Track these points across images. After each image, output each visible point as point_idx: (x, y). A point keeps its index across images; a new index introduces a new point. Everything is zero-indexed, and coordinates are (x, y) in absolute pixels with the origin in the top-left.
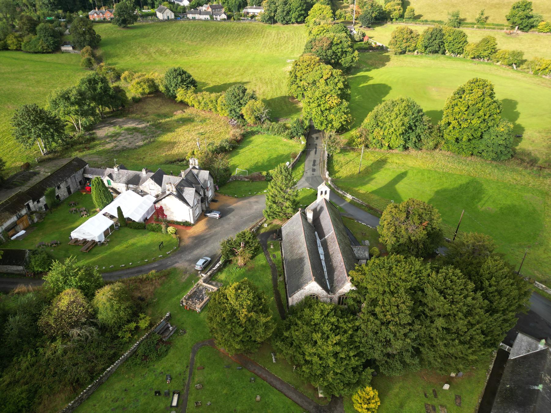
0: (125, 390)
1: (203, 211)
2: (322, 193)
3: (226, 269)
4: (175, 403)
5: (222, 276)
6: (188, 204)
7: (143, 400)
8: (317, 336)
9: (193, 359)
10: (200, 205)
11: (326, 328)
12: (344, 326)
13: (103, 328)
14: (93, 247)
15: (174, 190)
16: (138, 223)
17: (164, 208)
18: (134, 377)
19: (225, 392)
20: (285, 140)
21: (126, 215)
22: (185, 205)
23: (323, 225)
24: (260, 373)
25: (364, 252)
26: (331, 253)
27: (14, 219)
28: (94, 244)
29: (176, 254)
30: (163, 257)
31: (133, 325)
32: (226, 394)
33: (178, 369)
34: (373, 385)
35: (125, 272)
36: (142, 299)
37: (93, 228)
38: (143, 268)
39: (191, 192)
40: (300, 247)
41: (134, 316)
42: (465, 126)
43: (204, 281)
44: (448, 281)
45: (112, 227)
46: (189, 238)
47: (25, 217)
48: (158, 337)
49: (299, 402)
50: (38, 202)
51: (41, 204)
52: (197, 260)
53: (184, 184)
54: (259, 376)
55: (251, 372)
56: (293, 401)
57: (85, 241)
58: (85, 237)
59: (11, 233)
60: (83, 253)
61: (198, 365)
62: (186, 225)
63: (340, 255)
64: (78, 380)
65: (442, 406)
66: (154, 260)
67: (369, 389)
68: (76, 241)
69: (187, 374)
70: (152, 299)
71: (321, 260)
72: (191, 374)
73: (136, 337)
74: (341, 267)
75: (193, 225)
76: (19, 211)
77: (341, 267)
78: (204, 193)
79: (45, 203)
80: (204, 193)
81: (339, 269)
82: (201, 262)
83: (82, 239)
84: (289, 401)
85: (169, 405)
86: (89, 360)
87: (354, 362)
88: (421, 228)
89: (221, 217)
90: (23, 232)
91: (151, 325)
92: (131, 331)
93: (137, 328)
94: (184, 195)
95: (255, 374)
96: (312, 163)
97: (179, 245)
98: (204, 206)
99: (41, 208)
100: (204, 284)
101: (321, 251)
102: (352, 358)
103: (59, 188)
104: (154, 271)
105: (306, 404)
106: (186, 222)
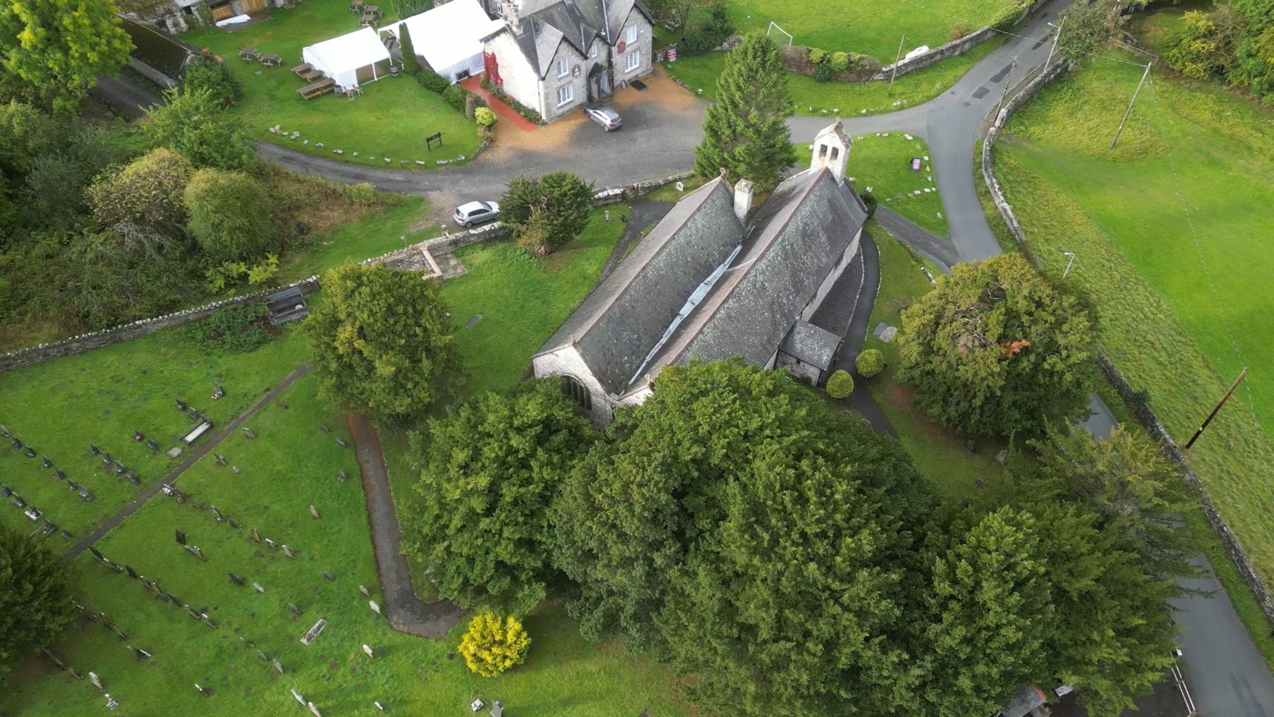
0: (145, 372)
1: (590, 98)
2: (824, 149)
3: (501, 246)
4: (190, 438)
5: (481, 257)
6: (536, 68)
7: (156, 403)
9: (289, 382)
10: (580, 81)
11: (491, 451)
12: (536, 469)
13: (195, 248)
14: (323, 94)
15: (516, 21)
16: (436, 76)
17: (498, 60)
18: (175, 358)
19: (279, 467)
21: (418, 51)
22: (528, 67)
24: (371, 473)
25: (821, 348)
28: (331, 88)
29: (453, 172)
30: (425, 167)
31: (237, 268)
32: (279, 472)
33: (249, 386)
34: (529, 624)
35: (336, 167)
36: (303, 230)
37: (344, 55)
38: (371, 173)
41: (253, 254)
43: (430, 250)
44: (787, 497)
45: (383, 65)
46: (510, 149)
48: (263, 309)
49: (383, 566)
52: (467, 199)
53: (557, 17)
54: (362, 476)
55: (357, 461)
56: (376, 556)
57: (320, 76)
58: (323, 69)
59: (221, 11)
60: (300, 99)
61: (286, 397)
62: (531, 118)
64: (86, 316)
66: (403, 167)
67: (514, 625)
68: (308, 69)
69: (259, 400)
70: (322, 238)
71: (675, 314)
72: (261, 405)
73: (232, 291)
75: (544, 124)
78: (610, 55)
80: (610, 55)
82: (466, 209)
83: (317, 68)
84: (367, 549)
85: (182, 435)
86: (123, 292)
87: (504, 552)
88: (998, 350)
89: (615, 129)
90: (244, 18)
91: (272, 282)
92: (227, 277)
93: (244, 277)
94: (538, 42)
95: (361, 469)
96: (998, 71)
97: (477, 155)
98: (595, 87)
100: (426, 254)
101: (698, 294)
102: (504, 543)
104: (366, 185)
105: (393, 575)
106: (534, 111)
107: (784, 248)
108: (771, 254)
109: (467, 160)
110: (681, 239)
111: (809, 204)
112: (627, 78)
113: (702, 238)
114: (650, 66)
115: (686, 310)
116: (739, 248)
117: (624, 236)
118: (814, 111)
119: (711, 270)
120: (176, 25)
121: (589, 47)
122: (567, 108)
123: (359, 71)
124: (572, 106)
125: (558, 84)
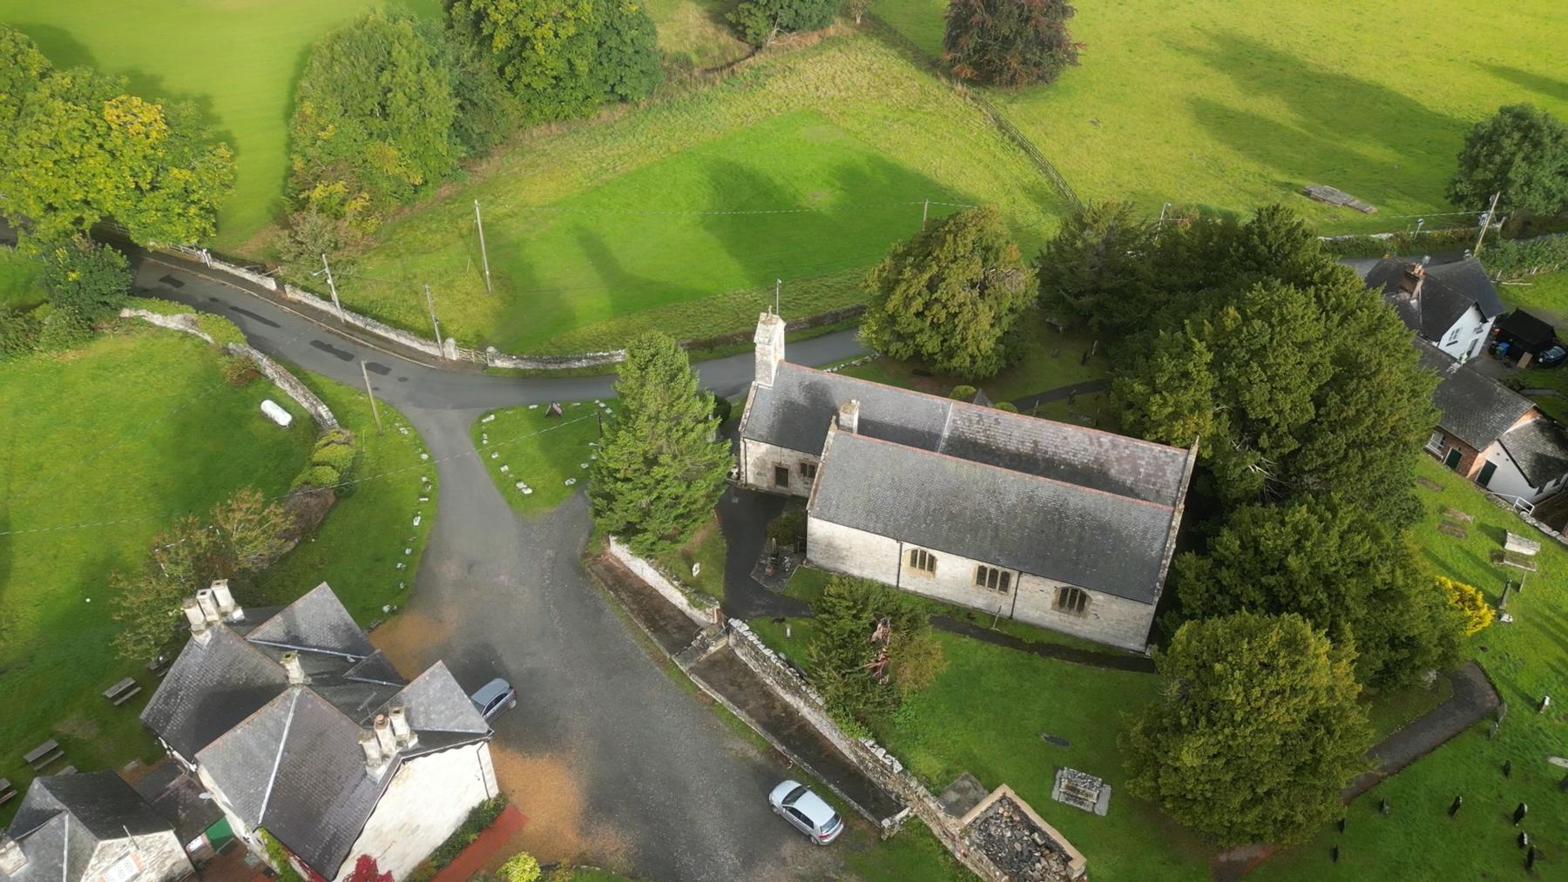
8: (1382, 575)
17: (375, 854)
20: (71, 355)
23: (888, 419)
26: (1027, 448)
39: (438, 684)
40: (992, 492)
42: (572, 31)
46: (584, 831)
63: (1070, 430)
65: (1443, 510)
74: (1115, 446)
77: (1115, 446)
81: (1113, 454)
84: (1447, 751)
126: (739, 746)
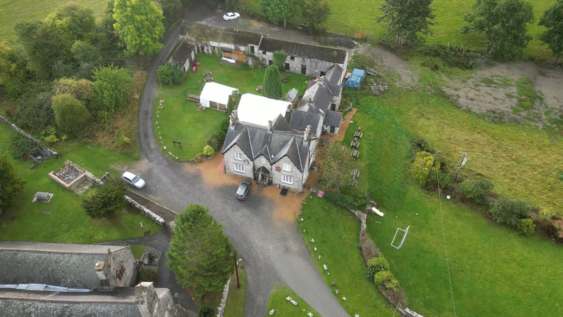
27: (232, 46)
47: (241, 53)
50: (264, 53)
51: (264, 56)
71: (16, 282)
76: (240, 44)
79: (271, 59)
90: (233, 61)
97: (186, 162)
99: (264, 59)
103: (292, 58)
107: (63, 311)
108: (52, 306)
109: (178, 160)
110: (44, 256)
111: (108, 307)
112: (282, 184)
113: (68, 267)
114: (301, 189)
115: (22, 286)
116: (87, 290)
117: (134, 239)
118: (333, 286)
119: (58, 283)
120: (208, 50)
121: (258, 157)
122: (237, 173)
123: (211, 103)
124: (243, 175)
125: (235, 161)
126: (158, 199)
